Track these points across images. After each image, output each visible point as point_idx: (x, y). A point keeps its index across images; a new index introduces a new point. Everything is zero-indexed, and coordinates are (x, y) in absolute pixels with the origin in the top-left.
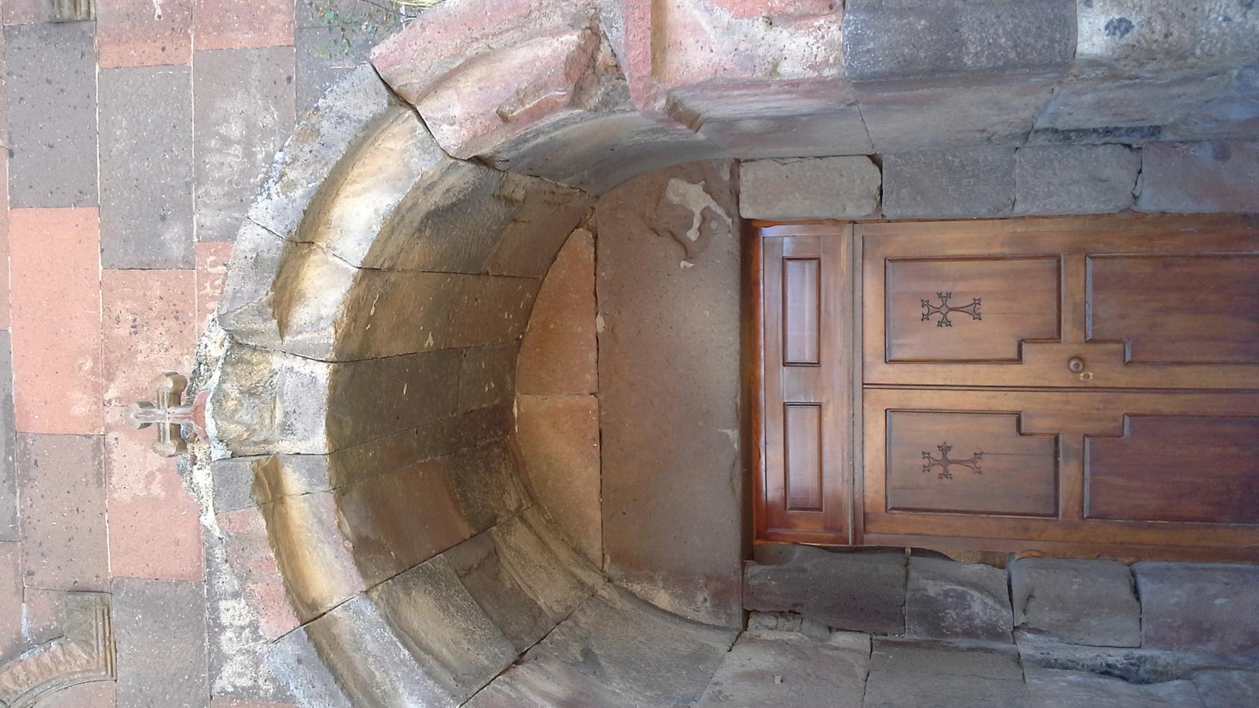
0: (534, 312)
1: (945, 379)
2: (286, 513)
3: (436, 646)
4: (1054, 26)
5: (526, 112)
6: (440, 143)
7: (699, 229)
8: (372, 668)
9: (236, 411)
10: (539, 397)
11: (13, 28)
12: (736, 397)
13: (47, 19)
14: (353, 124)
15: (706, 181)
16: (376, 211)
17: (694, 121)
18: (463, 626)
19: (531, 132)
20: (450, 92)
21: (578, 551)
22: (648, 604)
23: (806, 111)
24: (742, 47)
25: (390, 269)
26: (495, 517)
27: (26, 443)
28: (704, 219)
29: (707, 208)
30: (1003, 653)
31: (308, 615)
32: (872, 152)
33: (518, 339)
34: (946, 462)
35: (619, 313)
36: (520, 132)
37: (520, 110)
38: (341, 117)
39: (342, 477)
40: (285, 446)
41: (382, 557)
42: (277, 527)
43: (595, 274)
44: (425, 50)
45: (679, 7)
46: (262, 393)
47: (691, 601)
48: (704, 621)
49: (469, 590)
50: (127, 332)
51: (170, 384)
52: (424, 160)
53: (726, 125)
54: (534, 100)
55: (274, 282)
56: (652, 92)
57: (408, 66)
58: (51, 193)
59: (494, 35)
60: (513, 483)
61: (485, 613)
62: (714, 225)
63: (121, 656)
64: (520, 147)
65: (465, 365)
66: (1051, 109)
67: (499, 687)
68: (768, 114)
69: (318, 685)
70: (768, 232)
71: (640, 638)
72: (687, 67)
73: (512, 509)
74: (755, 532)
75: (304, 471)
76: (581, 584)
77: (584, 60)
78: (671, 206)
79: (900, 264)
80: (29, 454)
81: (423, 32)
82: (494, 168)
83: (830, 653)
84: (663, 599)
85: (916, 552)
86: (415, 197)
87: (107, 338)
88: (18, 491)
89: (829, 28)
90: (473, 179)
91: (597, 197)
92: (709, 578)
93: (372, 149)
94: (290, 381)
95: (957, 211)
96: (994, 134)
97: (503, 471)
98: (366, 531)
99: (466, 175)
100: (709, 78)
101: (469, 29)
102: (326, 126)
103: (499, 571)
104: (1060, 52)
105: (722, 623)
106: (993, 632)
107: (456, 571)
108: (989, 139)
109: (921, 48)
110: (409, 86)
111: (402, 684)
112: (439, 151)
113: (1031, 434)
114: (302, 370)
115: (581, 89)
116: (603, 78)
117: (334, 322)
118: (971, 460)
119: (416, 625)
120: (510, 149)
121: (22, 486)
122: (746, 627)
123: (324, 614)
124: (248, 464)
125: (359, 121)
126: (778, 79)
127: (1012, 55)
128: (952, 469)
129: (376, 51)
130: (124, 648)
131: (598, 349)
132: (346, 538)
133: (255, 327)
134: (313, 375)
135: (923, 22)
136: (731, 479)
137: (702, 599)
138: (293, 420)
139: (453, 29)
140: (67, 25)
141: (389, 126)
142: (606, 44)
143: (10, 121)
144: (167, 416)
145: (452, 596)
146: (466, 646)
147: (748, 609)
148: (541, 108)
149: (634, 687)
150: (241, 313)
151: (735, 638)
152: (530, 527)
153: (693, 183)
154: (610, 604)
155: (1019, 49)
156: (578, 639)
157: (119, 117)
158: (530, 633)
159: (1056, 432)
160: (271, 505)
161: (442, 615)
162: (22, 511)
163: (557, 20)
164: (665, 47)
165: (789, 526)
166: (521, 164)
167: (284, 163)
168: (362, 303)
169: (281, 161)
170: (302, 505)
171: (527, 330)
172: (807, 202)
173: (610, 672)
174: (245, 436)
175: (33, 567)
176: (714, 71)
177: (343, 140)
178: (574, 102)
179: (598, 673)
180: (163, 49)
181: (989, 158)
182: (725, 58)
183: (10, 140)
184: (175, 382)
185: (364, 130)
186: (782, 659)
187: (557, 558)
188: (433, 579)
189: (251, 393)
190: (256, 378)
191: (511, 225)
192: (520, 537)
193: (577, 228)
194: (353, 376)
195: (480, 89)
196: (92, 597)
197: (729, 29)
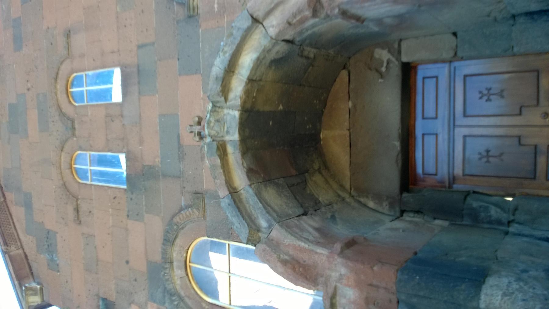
3: (273, 205)
5: (298, 21)
8: (251, 209)
9: (213, 127)
16: (251, 60)
21: (342, 187)
22: (365, 206)
25: (260, 80)
26: (308, 170)
27: (183, 148)
28: (388, 63)
31: (232, 191)
34: (488, 156)
36: (298, 29)
37: (294, 21)
38: (239, 29)
40: (227, 138)
51: (197, 119)
53: (379, 21)
61: (296, 199)
62: (391, 65)
69: (234, 212)
76: (339, 196)
84: (371, 204)
94: (228, 118)
99: (282, 48)
102: (235, 32)
103: (306, 187)
106: (499, 222)
119: (267, 198)
122: (402, 215)
128: (491, 159)
130: (208, 211)
132: (244, 167)
136: (397, 161)
152: (323, 176)
160: (222, 156)
162: (182, 169)
183: (178, 55)
184: (198, 118)
188: (277, 185)
189: (218, 121)
190: (219, 116)
196: (200, 195)
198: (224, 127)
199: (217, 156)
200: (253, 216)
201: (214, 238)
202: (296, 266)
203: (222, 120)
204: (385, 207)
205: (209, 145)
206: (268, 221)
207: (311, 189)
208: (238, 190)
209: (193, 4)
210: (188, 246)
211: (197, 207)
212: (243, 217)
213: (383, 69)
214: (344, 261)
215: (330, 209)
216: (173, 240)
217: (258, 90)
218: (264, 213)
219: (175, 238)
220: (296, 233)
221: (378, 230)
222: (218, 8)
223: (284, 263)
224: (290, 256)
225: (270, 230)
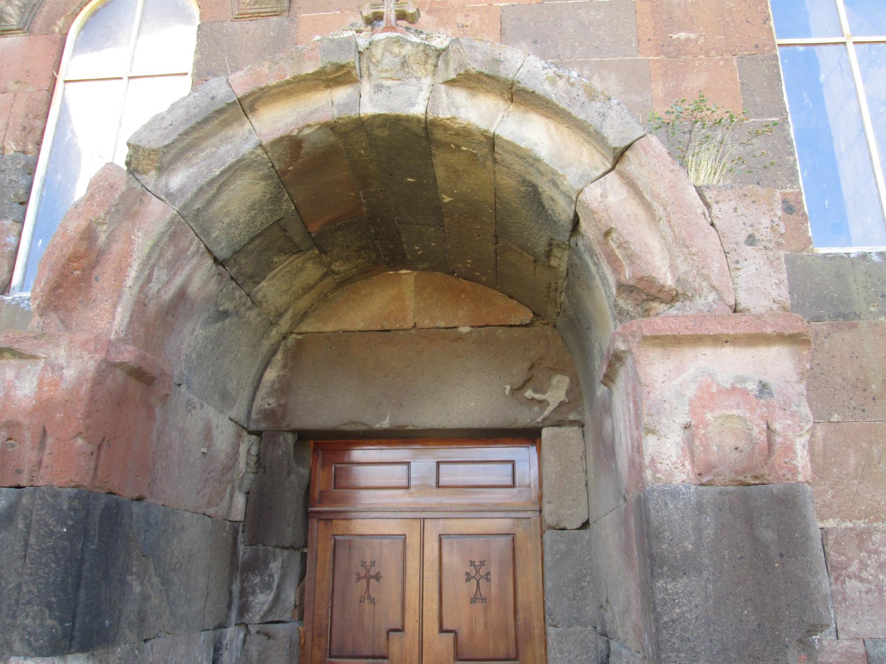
0: (473, 283)
1: (428, 577)
2: (319, 90)
3: (224, 197)
4: (690, 652)
5: (612, 251)
7: (533, 399)
8: (208, 150)
9: (391, 53)
10: (413, 288)
12: (412, 426)
14: (599, 124)
15: (568, 403)
16: (536, 144)
17: (609, 379)
18: (241, 221)
19: (598, 259)
20: (626, 194)
21: (305, 315)
22: (266, 364)
23: (620, 464)
24: (666, 405)
25: (495, 161)
26: (326, 253)
28: (540, 402)
29: (548, 404)
30: (228, 616)
31: (246, 104)
32: (591, 521)
33: (454, 273)
34: (368, 578)
35: (473, 343)
36: (598, 249)
37: (613, 245)
39: (344, 128)
40: (366, 87)
41: (288, 160)
42: (308, 83)
44: (656, 172)
45: (696, 356)
46: (404, 71)
47: (269, 394)
48: (255, 403)
50: (459, 22)
52: (575, 176)
53: (607, 408)
54: (622, 255)
55: (483, 73)
56: (630, 338)
57: (643, 161)
59: (669, 222)
60: (351, 269)
61: (253, 239)
62: (536, 409)
63: (248, 23)
64: (587, 252)
65: (432, 229)
66: (624, 652)
67: (195, 243)
68: (616, 436)
69: (196, 111)
70: (533, 450)
71: (239, 355)
72: (650, 364)
73: (333, 267)
74: (319, 442)
75: (348, 101)
76: (280, 316)
77: (653, 291)
79: (511, 545)
81: (669, 171)
82: (571, 236)
83: (228, 491)
84: (271, 375)
85: (304, 556)
86: (547, 173)
87: (455, 10)
89: (684, 473)
90: (562, 219)
91: (555, 326)
92: (284, 407)
93: (582, 140)
94: (412, 89)
95: (549, 584)
96: (606, 610)
97: (360, 261)
98: (306, 147)
99: (563, 211)
100: (642, 380)
101: (673, 203)
102: (597, 105)
103: (286, 253)
104: (669, 657)
105: (254, 416)
106: (244, 609)
107: (282, 218)
108: (601, 607)
109: (670, 545)
110: (629, 163)
111: (196, 171)
112: (581, 187)
113: (388, 639)
114: (420, 97)
115: (631, 291)
116: (639, 309)
117: (454, 118)
118: (369, 597)
119: (238, 182)
120: (585, 246)
122: (250, 433)
123: (248, 118)
124: (353, 60)
125: (601, 127)
126: (643, 434)
127: (666, 619)
128: (365, 581)
129: (653, 139)
131: (447, 328)
132: (300, 131)
133: (451, 64)
135: (690, 547)
136: (354, 423)
137: (270, 402)
138: (385, 92)
139: (672, 192)
141: (598, 151)
142: (666, 308)
144: (389, 10)
145: (263, 213)
147: (263, 435)
148: (615, 261)
149: (199, 346)
150: (460, 53)
151: (241, 424)
152: (320, 280)
153: (567, 394)
154: (266, 336)
155: (671, 623)
156: (237, 309)
157: (602, 14)
158: (239, 272)
159: (390, 657)
163: (683, 268)
164: (665, 346)
165: (323, 466)
166: (575, 258)
168: (469, 139)
169: (570, 75)
170: (324, 101)
171: (460, 279)
172: (553, 476)
173: (211, 329)
174: (374, 60)
176: (647, 384)
177: (587, 117)
179: (210, 320)
180: (649, 40)
181: (588, 608)
182: (658, 393)
184: (413, 15)
185: (595, 131)
186: (223, 455)
188: (275, 200)
190: (415, 67)
191: (532, 258)
192: (312, 272)
193: (533, 313)
194: (417, 135)
195: (628, 215)
198: (391, 78)
199: (321, 65)
200: (194, 155)
202: (84, 262)
203: (408, 72)
204: (265, 401)
206: (181, 190)
207: (285, 264)
208: (250, 116)
212: (186, 133)
213: (529, 394)
214: (90, 375)
215: (245, 305)
217: (475, 155)
218: (199, 181)
220: (160, 256)
221: (202, 406)
222: (678, 39)
223: (89, 235)
224: (108, 244)
225: (163, 197)
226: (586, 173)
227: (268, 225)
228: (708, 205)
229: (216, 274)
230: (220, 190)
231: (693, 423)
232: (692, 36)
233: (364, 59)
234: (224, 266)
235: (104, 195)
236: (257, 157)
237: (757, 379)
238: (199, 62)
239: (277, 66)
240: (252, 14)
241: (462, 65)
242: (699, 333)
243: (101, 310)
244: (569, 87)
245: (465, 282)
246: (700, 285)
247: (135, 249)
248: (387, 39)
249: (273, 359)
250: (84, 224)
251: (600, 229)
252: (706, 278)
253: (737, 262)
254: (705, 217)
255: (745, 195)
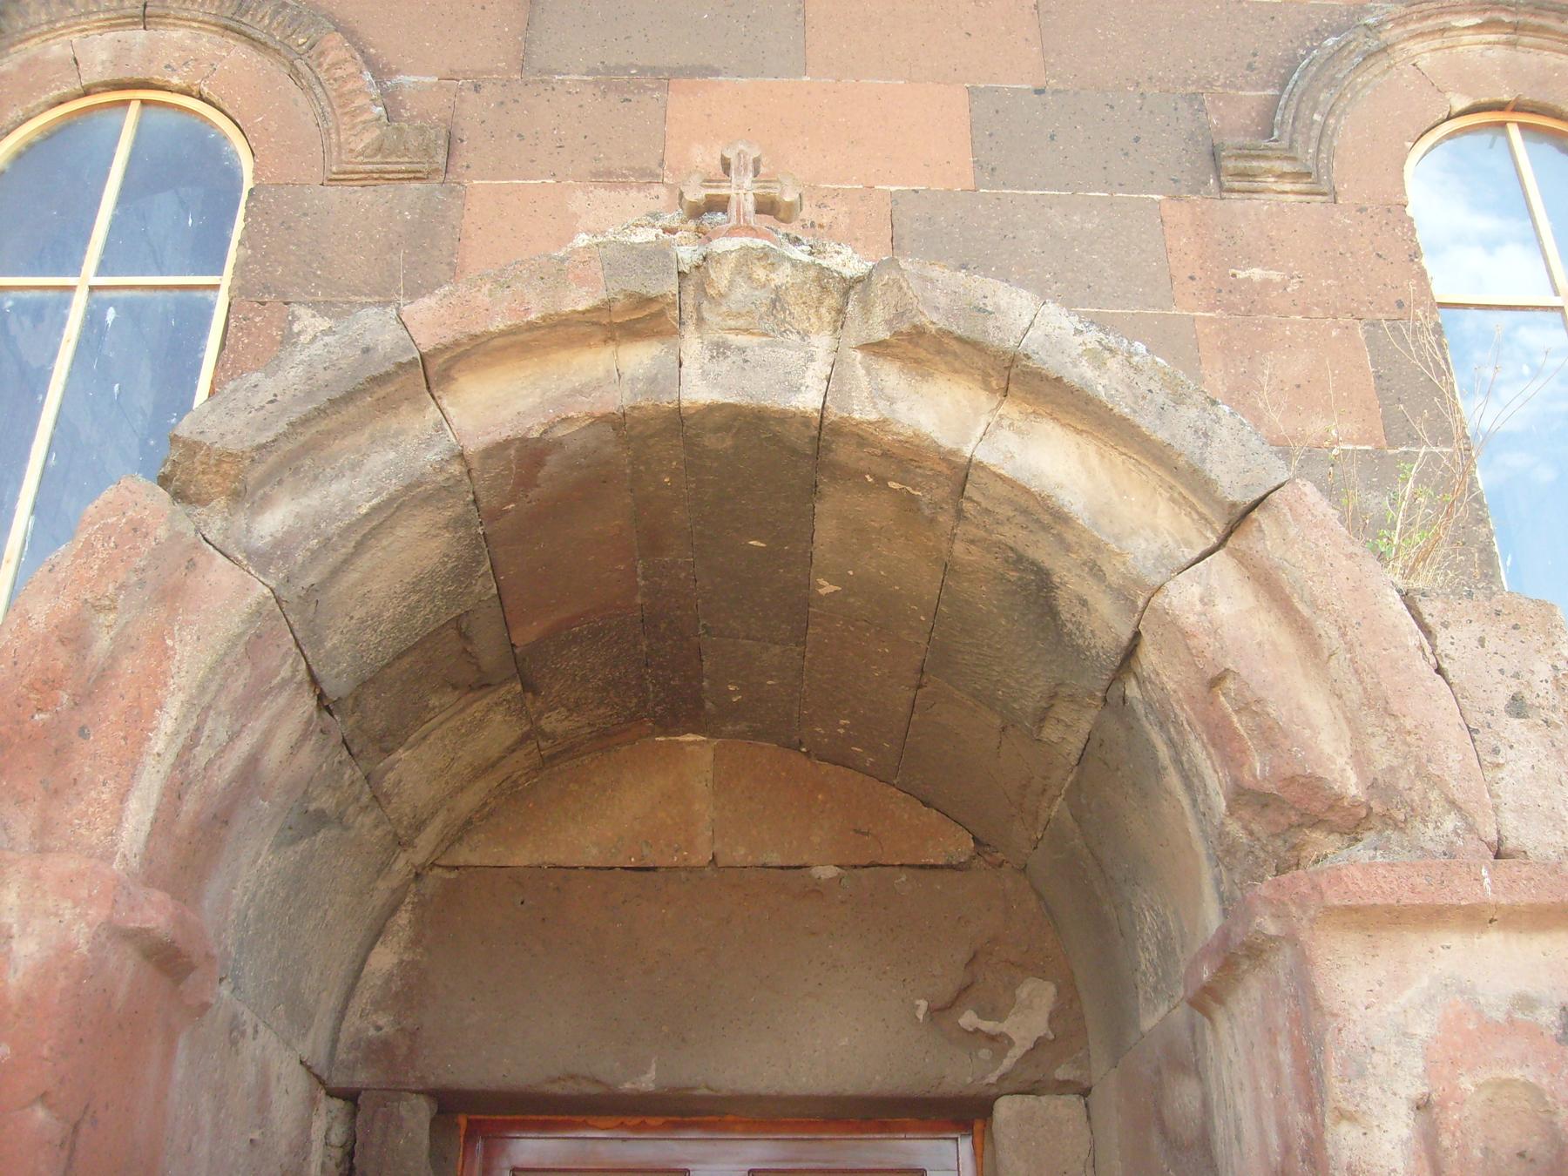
0: (842, 769)
2: (590, 346)
3: (364, 562)
6: (1172, 583)
7: (977, 1030)
10: (710, 776)
11: (1202, 103)
12: (708, 1087)
13: (1216, 142)
14: (1198, 451)
15: (1054, 1040)
16: (1060, 486)
18: (386, 615)
19: (1180, 733)
21: (464, 830)
22: (377, 933)
24: (1376, 1058)
25: (960, 514)
26: (536, 693)
27: (653, 90)
28: (992, 1038)
29: (1011, 1043)
31: (435, 366)
33: (801, 743)
36: (1184, 713)
40: (693, 346)
41: (509, 488)
42: (571, 329)
43: (901, 865)
44: (1320, 559)
45: (1431, 952)
47: (377, 1005)
48: (345, 1025)
49: (437, 632)
56: (1293, 909)
58: (991, 135)
61: (400, 656)
62: (985, 1053)
65: (777, 649)
69: (328, 375)
70: (965, 1146)
71: (331, 913)
74: (479, 1117)
76: (419, 826)
77: (1317, 806)
78: (1012, 986)
80: (639, 93)
81: (1346, 556)
86: (1082, 546)
88: (590, 78)
90: (1099, 644)
92: (414, 1034)
94: (792, 357)
97: (601, 711)
100: (1322, 1002)
102: (1190, 413)
105: (342, 1055)
110: (1261, 535)
114: (810, 373)
115: (1265, 806)
116: (1279, 843)
117: (885, 421)
119: (400, 532)
121: (596, 83)
122: (332, 1093)
125: (1203, 461)
129: (1309, 489)
130: (367, 196)
134: (803, 388)
136: (573, 1077)
137: (381, 1023)
138: (734, 358)
139: (1355, 600)
140: (1212, 164)
143: (1082, 92)
146: (357, 615)
147: (361, 1098)
150: (901, 288)
151: (317, 1071)
152: (512, 750)
153: (1050, 1021)
157: (1097, 220)
158: (359, 728)
161: (407, 580)
162: (563, 82)
164: (1368, 929)
167: (1131, 355)
169: (1132, 349)
170: (600, 368)
173: (289, 853)
174: (711, 291)
175: (485, 92)
176: (1335, 1011)
178: (1244, 797)
180: (1192, 278)
183: (1056, 92)
184: (790, 205)
185: (1190, 465)
186: (283, 1147)
187: (462, 789)
188: (463, 572)
190: (796, 310)
195: (1260, 644)
196: (441, 158)
197: (1405, 1035)
198: (747, 331)
199: (603, 295)
201: (245, 220)
203: (784, 321)
205: (656, 255)
209: (1268, 172)
210: (215, 98)
211: (386, 142)
212: (306, 421)
213: (968, 1019)
215: (357, 799)
216: (243, 28)
219: (252, 41)
220: (222, 687)
222: (1249, 280)
226: (1166, 551)
227: (436, 625)
228: (1427, 631)
229: (318, 729)
230: (360, 547)
231: (1434, 1097)
232: (1275, 276)
233: (690, 289)
234: (332, 716)
235: (116, 546)
236: (448, 479)
237: (1556, 1002)
238: (247, 264)
239: (507, 292)
240: (413, 172)
241: (903, 314)
242: (1440, 902)
243: (90, 804)
244: (1131, 373)
245: (826, 767)
246: (1425, 797)
247: (174, 670)
248: (742, 252)
249: (389, 924)
250: (66, 605)
251: (1199, 671)
252: (1435, 782)
253: (1496, 751)
254: (1424, 654)
255: (1498, 613)
